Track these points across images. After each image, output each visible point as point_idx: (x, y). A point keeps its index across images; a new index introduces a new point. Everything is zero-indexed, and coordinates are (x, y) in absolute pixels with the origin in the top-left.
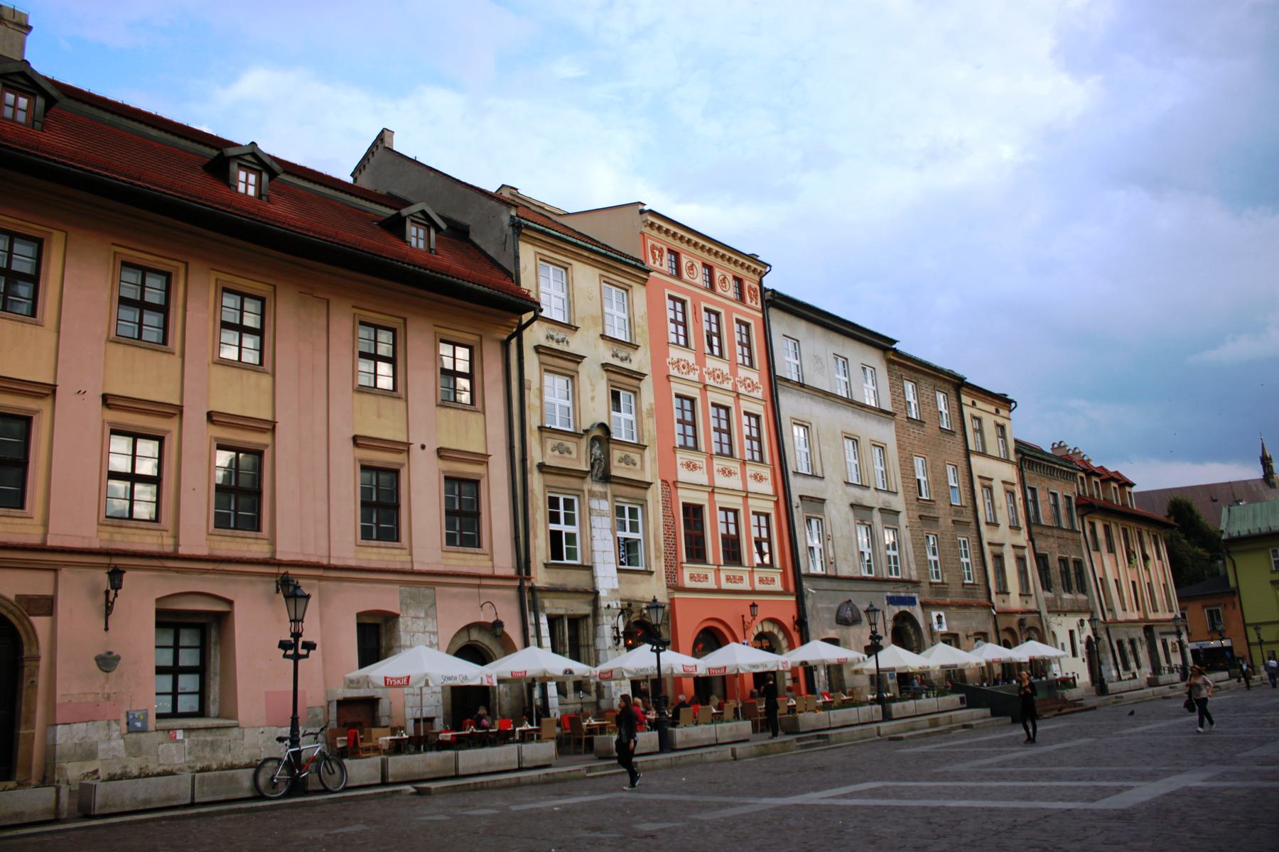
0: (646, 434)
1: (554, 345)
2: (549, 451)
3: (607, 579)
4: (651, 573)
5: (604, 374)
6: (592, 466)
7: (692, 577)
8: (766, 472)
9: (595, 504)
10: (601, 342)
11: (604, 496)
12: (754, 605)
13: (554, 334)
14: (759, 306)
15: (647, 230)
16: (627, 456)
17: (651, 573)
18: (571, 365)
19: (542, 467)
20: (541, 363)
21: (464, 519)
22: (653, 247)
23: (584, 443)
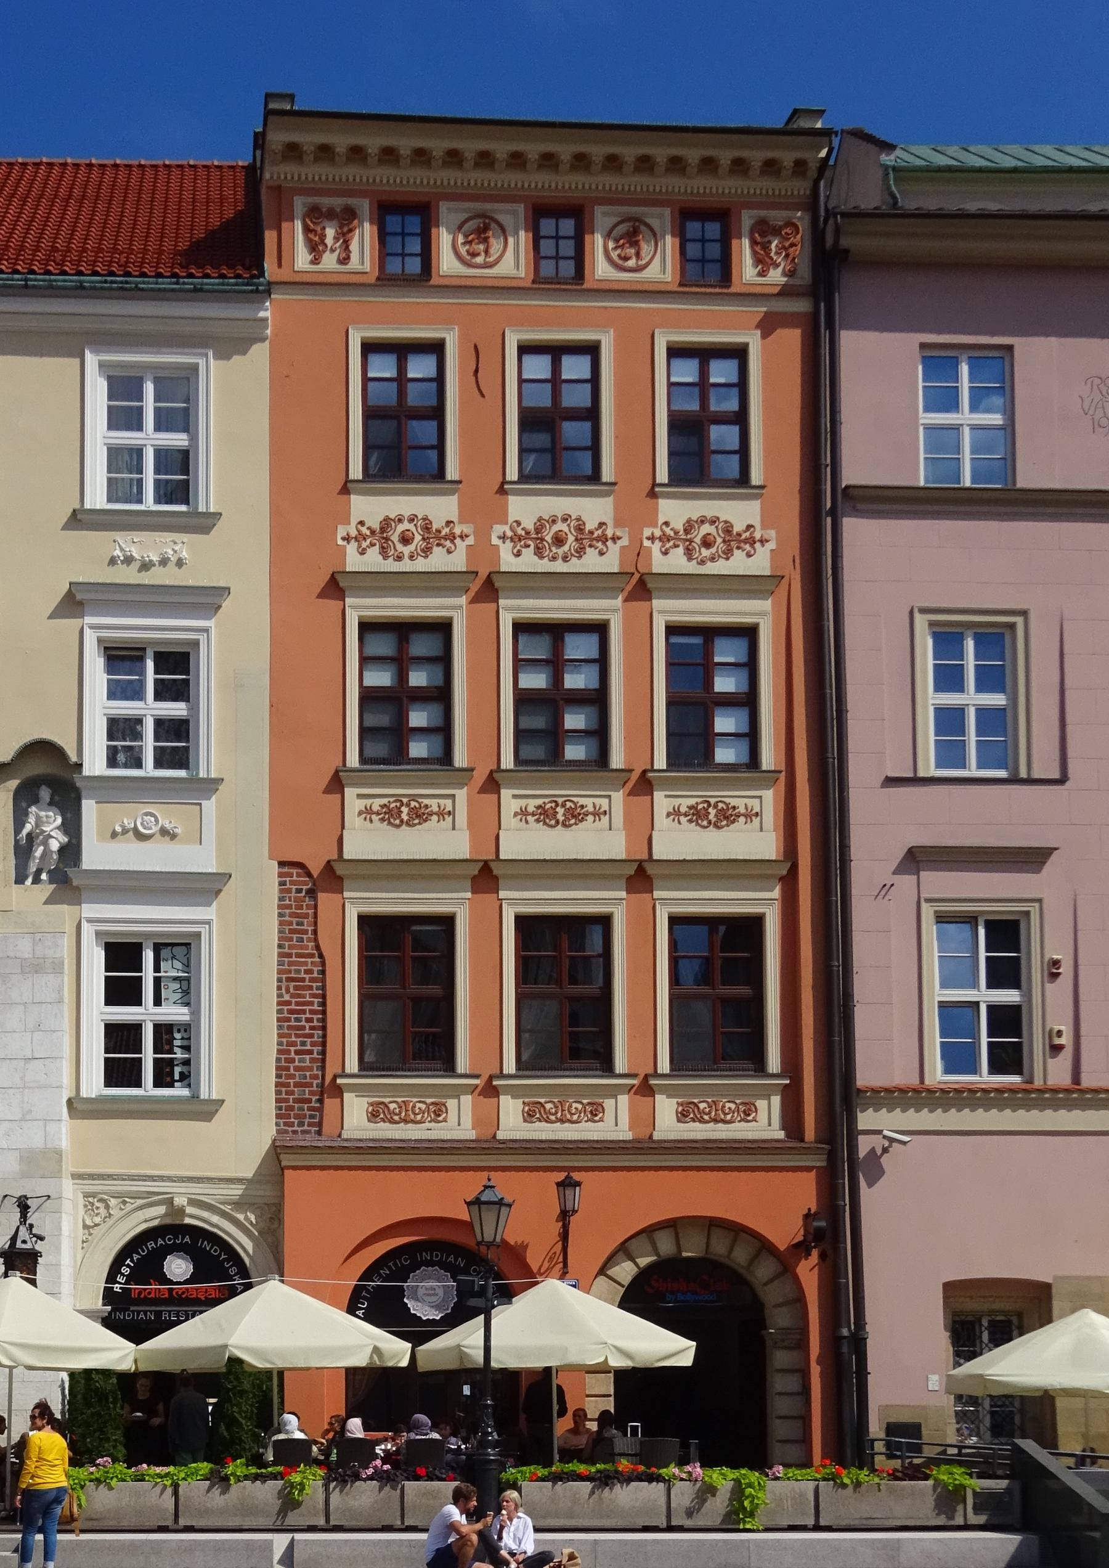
6: (23, 851)
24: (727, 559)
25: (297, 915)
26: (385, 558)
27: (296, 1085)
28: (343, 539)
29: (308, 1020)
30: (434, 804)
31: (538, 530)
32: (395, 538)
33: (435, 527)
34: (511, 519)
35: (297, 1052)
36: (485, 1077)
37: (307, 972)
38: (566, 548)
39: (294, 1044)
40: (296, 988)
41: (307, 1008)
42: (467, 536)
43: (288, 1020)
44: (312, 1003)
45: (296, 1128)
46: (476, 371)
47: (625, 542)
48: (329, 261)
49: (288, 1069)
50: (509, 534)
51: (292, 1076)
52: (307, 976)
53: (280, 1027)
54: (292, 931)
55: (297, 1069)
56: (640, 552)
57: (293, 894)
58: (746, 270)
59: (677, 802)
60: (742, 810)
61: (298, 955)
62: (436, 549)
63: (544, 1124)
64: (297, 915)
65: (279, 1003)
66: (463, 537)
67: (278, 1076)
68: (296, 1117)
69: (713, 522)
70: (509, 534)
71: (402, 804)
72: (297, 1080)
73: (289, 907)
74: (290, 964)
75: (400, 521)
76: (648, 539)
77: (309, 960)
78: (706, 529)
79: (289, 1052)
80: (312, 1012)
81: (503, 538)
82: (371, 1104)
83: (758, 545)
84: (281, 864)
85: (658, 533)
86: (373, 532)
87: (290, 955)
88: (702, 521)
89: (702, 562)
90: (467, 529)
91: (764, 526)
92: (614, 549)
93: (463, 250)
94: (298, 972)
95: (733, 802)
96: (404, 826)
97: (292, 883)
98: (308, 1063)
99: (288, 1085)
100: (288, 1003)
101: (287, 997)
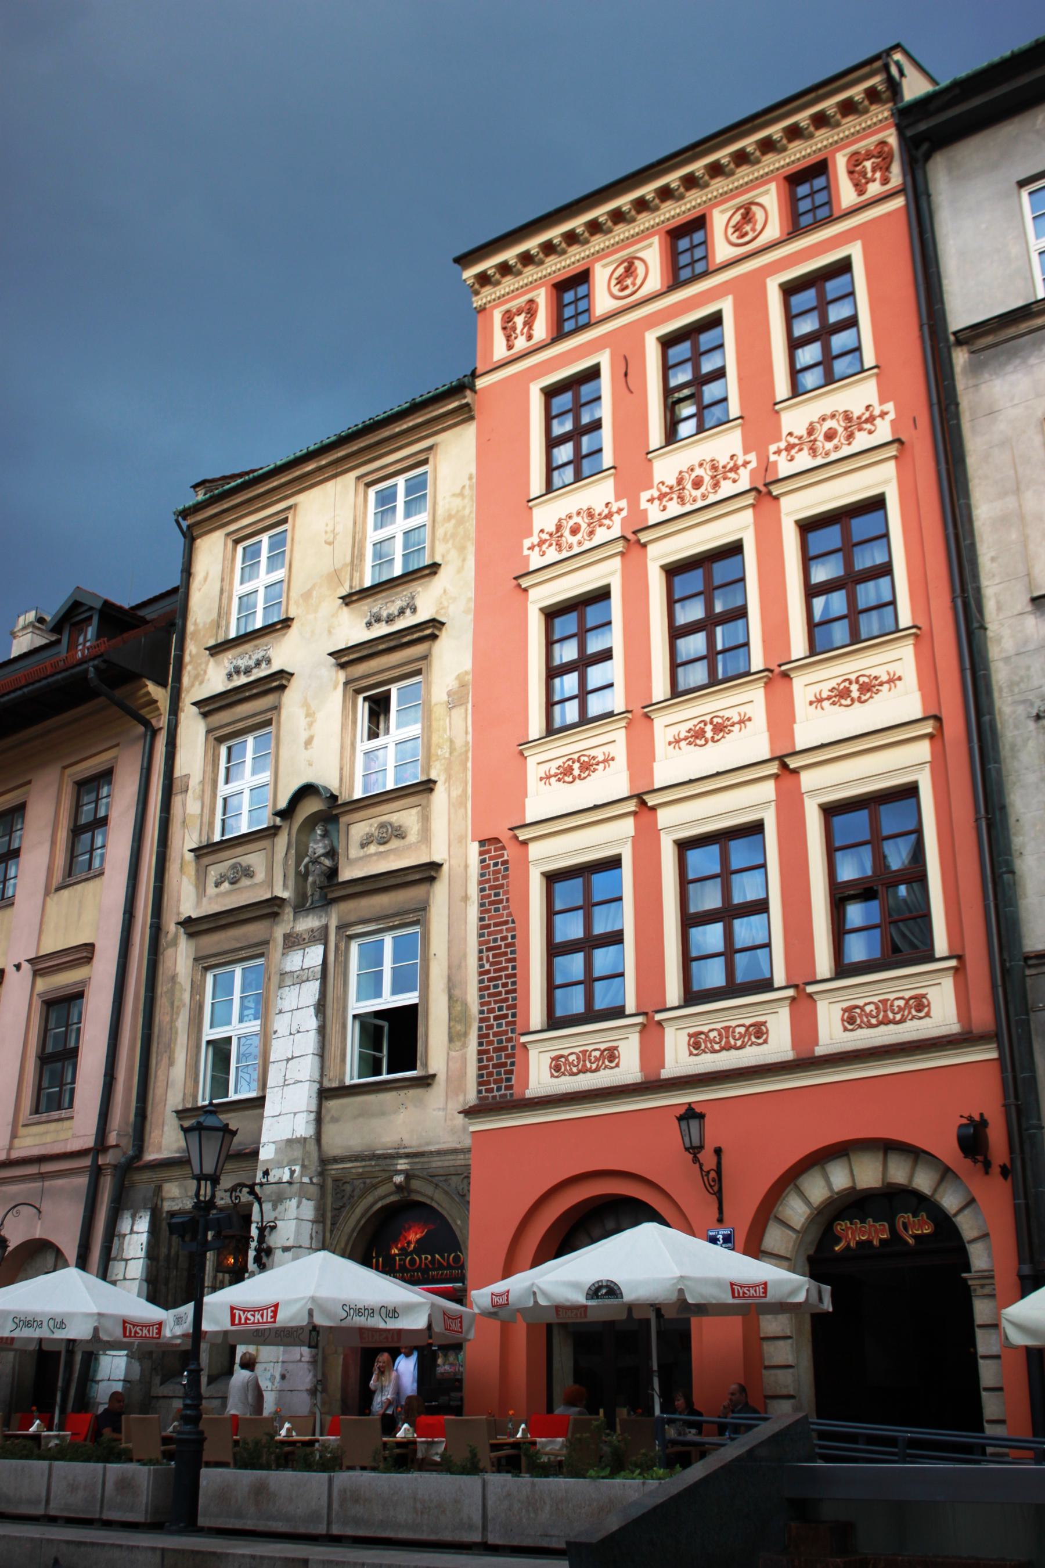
3: (286, 1117)
5: (341, 676)
9: (294, 961)
12: (690, 1115)
14: (896, 178)
15: (488, 294)
19: (192, 927)
21: (256, 1041)
22: (508, 317)
30: (599, 754)
31: (680, 481)
32: (566, 532)
35: (496, 1018)
38: (702, 489)
40: (494, 956)
41: (503, 974)
43: (488, 988)
44: (506, 968)
45: (495, 1093)
46: (626, 375)
47: (754, 464)
49: (487, 1035)
51: (490, 1043)
52: (503, 943)
53: (481, 997)
54: (491, 903)
55: (495, 1034)
56: (767, 466)
59: (815, 689)
61: (496, 925)
67: (480, 1044)
68: (496, 1082)
69: (833, 416)
72: (496, 1045)
73: (488, 881)
75: (570, 517)
76: (775, 453)
77: (504, 927)
80: (508, 977)
81: (651, 500)
83: (878, 421)
84: (482, 843)
86: (551, 535)
87: (488, 926)
89: (827, 454)
90: (623, 503)
91: (882, 401)
94: (495, 940)
95: (874, 672)
96: (577, 781)
98: (504, 1028)
99: (487, 1052)
100: (488, 972)
101: (487, 967)
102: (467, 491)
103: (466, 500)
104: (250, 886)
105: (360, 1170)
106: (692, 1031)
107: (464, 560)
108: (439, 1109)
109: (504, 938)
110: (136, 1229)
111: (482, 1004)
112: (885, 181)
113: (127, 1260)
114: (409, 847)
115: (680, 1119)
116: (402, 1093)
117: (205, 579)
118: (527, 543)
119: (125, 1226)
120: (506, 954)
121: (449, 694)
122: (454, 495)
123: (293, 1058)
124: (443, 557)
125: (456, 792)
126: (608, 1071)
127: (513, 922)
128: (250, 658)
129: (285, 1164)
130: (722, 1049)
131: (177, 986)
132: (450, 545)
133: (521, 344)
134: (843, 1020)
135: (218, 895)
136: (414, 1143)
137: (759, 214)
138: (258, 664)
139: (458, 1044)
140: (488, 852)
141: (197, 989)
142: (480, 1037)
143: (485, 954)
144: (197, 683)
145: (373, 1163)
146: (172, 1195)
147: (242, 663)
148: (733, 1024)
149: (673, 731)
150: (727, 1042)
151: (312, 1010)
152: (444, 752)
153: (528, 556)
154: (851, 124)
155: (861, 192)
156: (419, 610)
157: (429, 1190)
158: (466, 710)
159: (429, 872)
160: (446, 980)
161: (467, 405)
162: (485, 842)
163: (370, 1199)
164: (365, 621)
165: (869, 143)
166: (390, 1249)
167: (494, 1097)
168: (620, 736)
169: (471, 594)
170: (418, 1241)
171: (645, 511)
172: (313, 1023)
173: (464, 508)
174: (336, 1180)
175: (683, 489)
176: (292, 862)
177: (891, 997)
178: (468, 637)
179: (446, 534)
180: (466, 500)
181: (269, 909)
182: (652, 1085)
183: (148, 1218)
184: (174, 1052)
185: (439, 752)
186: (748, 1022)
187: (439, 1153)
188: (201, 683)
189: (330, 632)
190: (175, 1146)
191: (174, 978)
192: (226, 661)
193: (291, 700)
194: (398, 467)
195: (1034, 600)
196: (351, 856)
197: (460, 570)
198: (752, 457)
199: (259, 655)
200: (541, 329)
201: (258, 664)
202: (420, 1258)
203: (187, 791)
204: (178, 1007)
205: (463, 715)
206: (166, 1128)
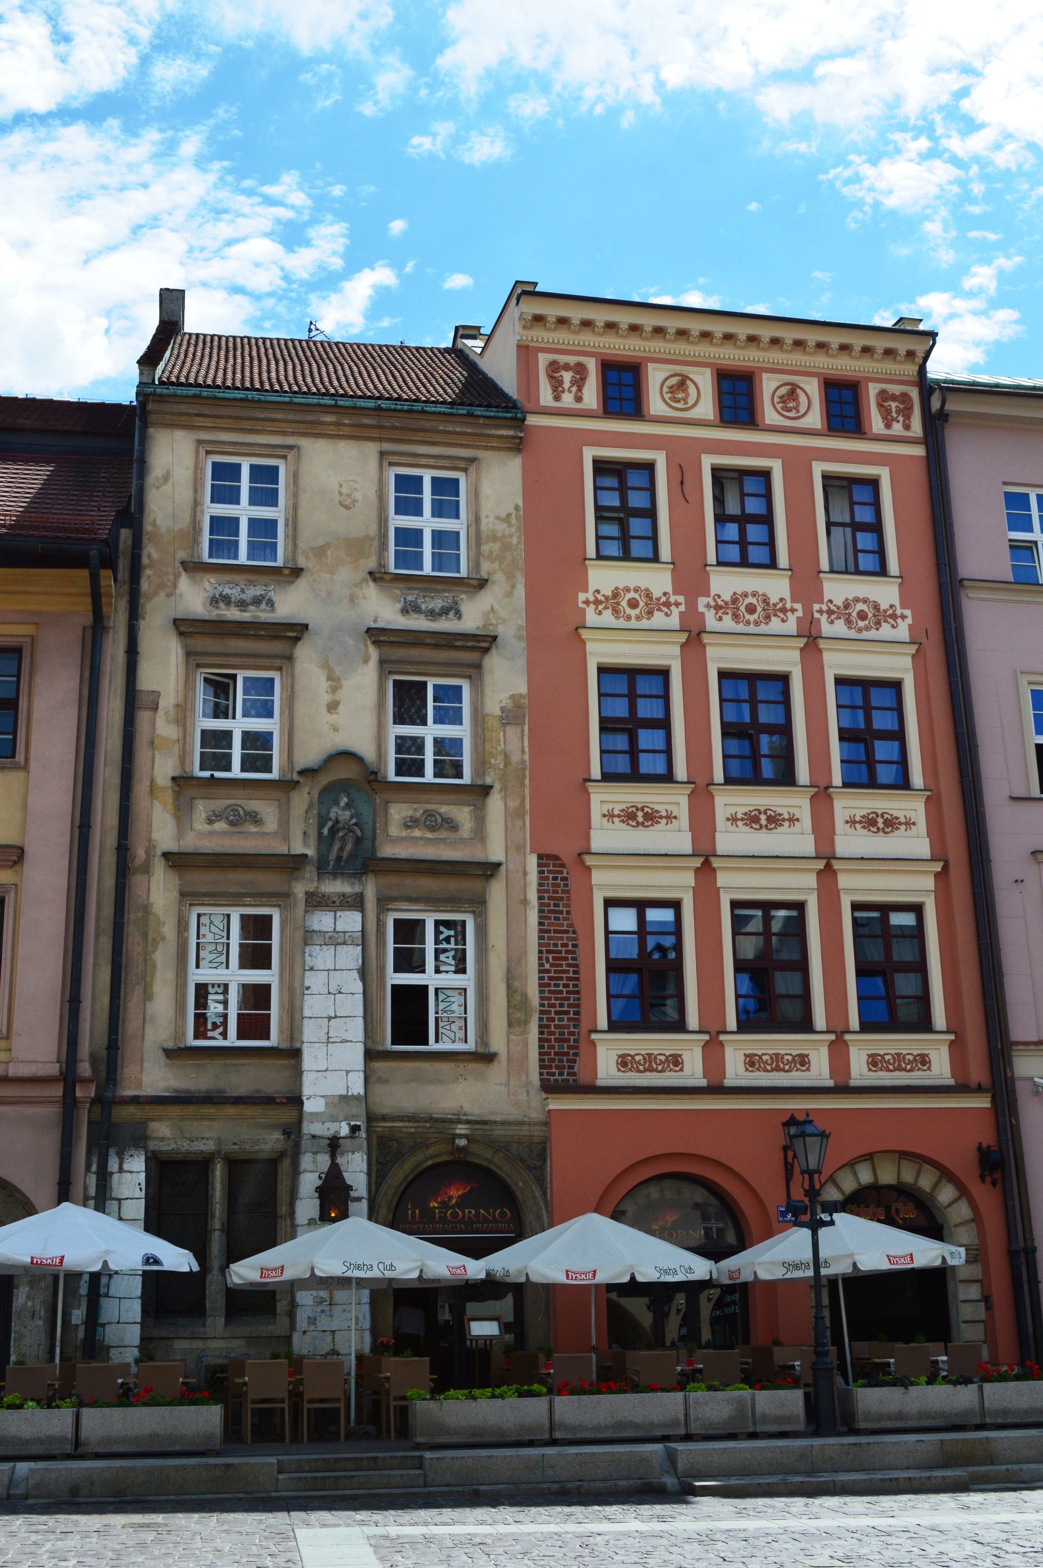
0: (498, 761)
1: (233, 614)
2: (200, 825)
4: (486, 1057)
5: (374, 653)
6: (324, 842)
7: (624, 1062)
8: (911, 807)
9: (323, 921)
10: (371, 590)
11: (357, 903)
13: (227, 591)
16: (429, 814)
17: (486, 1057)
18: (277, 647)
19: (176, 860)
20: (189, 654)
22: (554, 367)
23: (301, 800)
24: (877, 629)
25: (555, 899)
26: (617, 618)
27: (556, 1040)
28: (583, 602)
29: (566, 986)
30: (662, 810)
32: (624, 603)
33: (655, 596)
34: (712, 593)
35: (557, 1013)
36: (713, 1032)
37: (563, 945)
38: (756, 616)
39: (553, 1006)
40: (554, 958)
42: (680, 604)
43: (549, 985)
44: (567, 972)
45: (557, 1077)
46: (682, 483)
47: (800, 613)
48: (568, 400)
49: (549, 1027)
50: (712, 603)
51: (553, 1033)
52: (563, 949)
53: (541, 992)
55: (556, 1026)
57: (551, 881)
58: (876, 423)
60: (903, 820)
61: (555, 931)
62: (656, 613)
63: (762, 1073)
64: (555, 899)
65: (540, 971)
66: (677, 604)
67: (541, 1033)
68: (557, 1067)
70: (712, 603)
71: (637, 809)
73: (548, 891)
74: (549, 938)
75: (628, 590)
77: (565, 936)
78: (860, 606)
79: (549, 1012)
80: (569, 979)
81: (708, 606)
82: (619, 1056)
83: (899, 620)
84: (540, 857)
85: (824, 608)
87: (549, 931)
88: (857, 600)
89: (860, 630)
90: (681, 599)
91: (903, 606)
92: (792, 619)
93: (667, 396)
97: (549, 872)
98: (565, 1022)
99: (549, 1040)
100: (548, 971)
101: (547, 966)
102: (514, 521)
103: (513, 530)
104: (257, 833)
105: (413, 1130)
106: (748, 1052)
107: (513, 587)
108: (501, 1084)
109: (566, 945)
110: (126, 1167)
111: (542, 999)
112: (907, 427)
113: (119, 1200)
114: (463, 840)
115: (784, 1124)
116: (461, 1065)
117: (166, 478)
118: (582, 597)
119: (113, 1164)
120: (566, 959)
121: (502, 709)
122: (498, 518)
123: (336, 1017)
124: (489, 573)
125: (513, 804)
126: (672, 1073)
127: (574, 932)
128: (243, 591)
129: (341, 1119)
130: (773, 1070)
131: (151, 917)
132: (496, 565)
133: (568, 400)
134: (868, 1063)
135: (211, 833)
136: (476, 1111)
137: (803, 398)
138: (257, 601)
139: (518, 1030)
140: (548, 865)
141: (182, 926)
142: (540, 1026)
143: (544, 955)
144: (162, 594)
145: (428, 1125)
146: (161, 1135)
147: (233, 592)
148: (783, 1052)
149: (732, 810)
150: (777, 1063)
151: (355, 975)
152: (498, 761)
153: (584, 609)
154: (889, 367)
155: (888, 426)
156: (464, 617)
157: (488, 1154)
158: (523, 731)
159: (490, 870)
160: (505, 971)
161: (521, 438)
162: (543, 858)
163: (419, 1156)
164: (399, 606)
165: (896, 389)
166: (429, 1202)
167: (556, 1081)
168: (684, 801)
169: (522, 621)
170: (459, 1197)
171: (703, 614)
172: (358, 987)
173: (511, 536)
174: (380, 1138)
175: (738, 609)
176: (313, 821)
177: (904, 1052)
178: (521, 663)
179: (491, 553)
180: (513, 530)
181: (294, 864)
182: (716, 1089)
183: (143, 1158)
184: (151, 986)
185: (493, 761)
186: (794, 1053)
187: (503, 1123)
188: (169, 595)
189: (352, 600)
190: (162, 1085)
191: (146, 908)
192: (207, 584)
193: (307, 657)
194: (432, 462)
195: (1014, 799)
196: (390, 833)
197: (509, 595)
198: (798, 606)
199: (258, 591)
200: (591, 397)
201: (257, 601)
202: (464, 1213)
203: (157, 709)
204: (154, 940)
205: (519, 735)
206: (146, 1065)
